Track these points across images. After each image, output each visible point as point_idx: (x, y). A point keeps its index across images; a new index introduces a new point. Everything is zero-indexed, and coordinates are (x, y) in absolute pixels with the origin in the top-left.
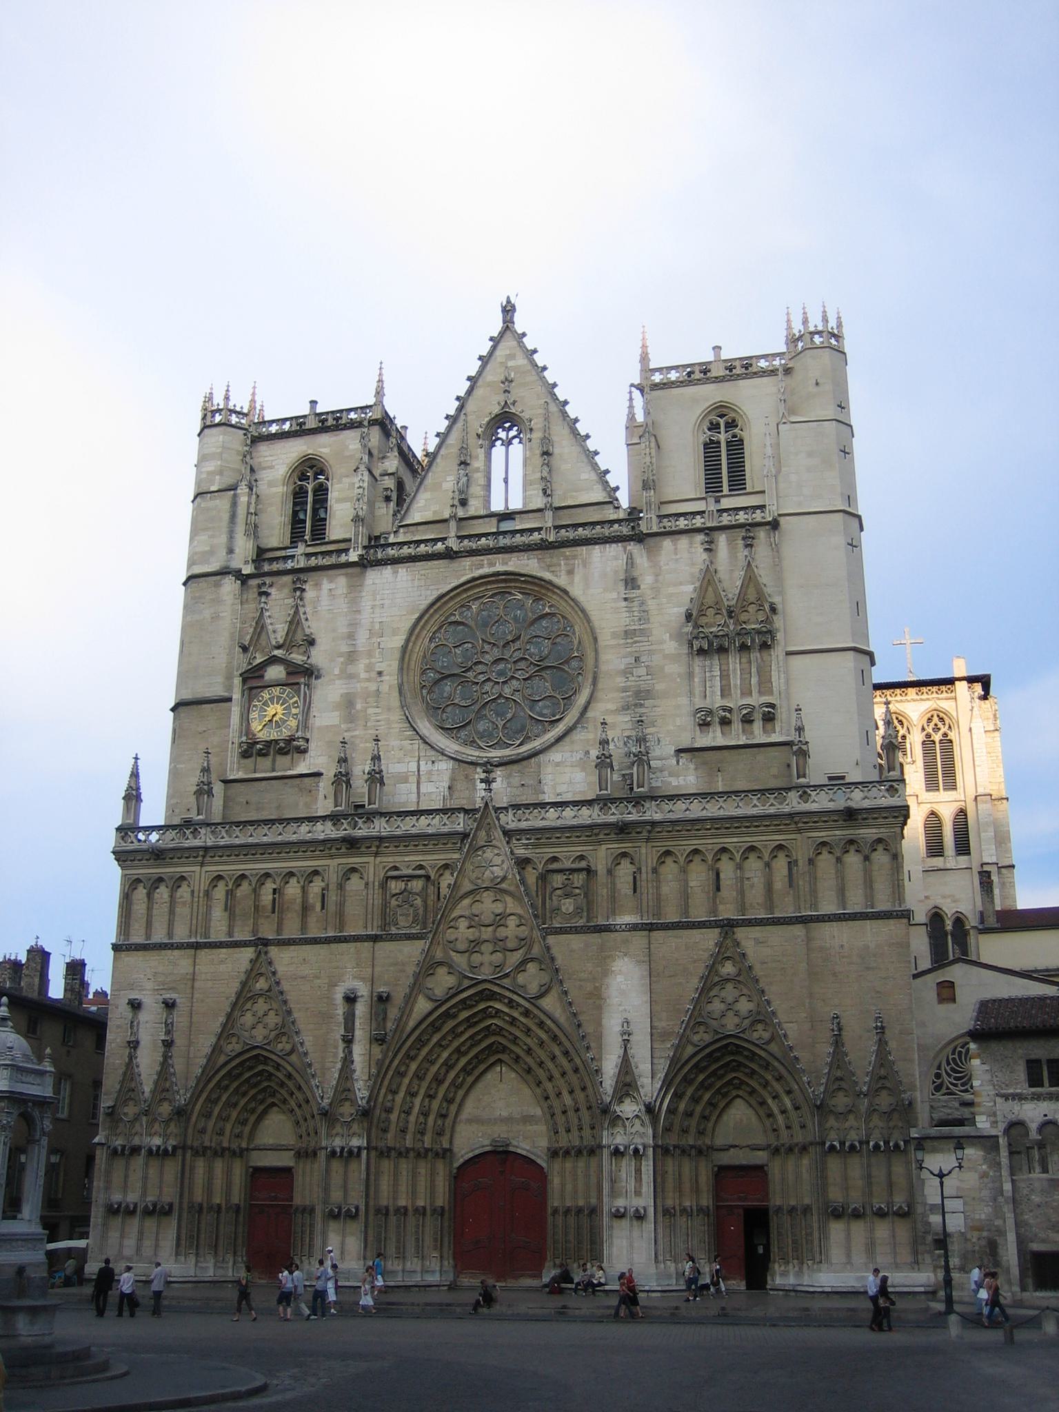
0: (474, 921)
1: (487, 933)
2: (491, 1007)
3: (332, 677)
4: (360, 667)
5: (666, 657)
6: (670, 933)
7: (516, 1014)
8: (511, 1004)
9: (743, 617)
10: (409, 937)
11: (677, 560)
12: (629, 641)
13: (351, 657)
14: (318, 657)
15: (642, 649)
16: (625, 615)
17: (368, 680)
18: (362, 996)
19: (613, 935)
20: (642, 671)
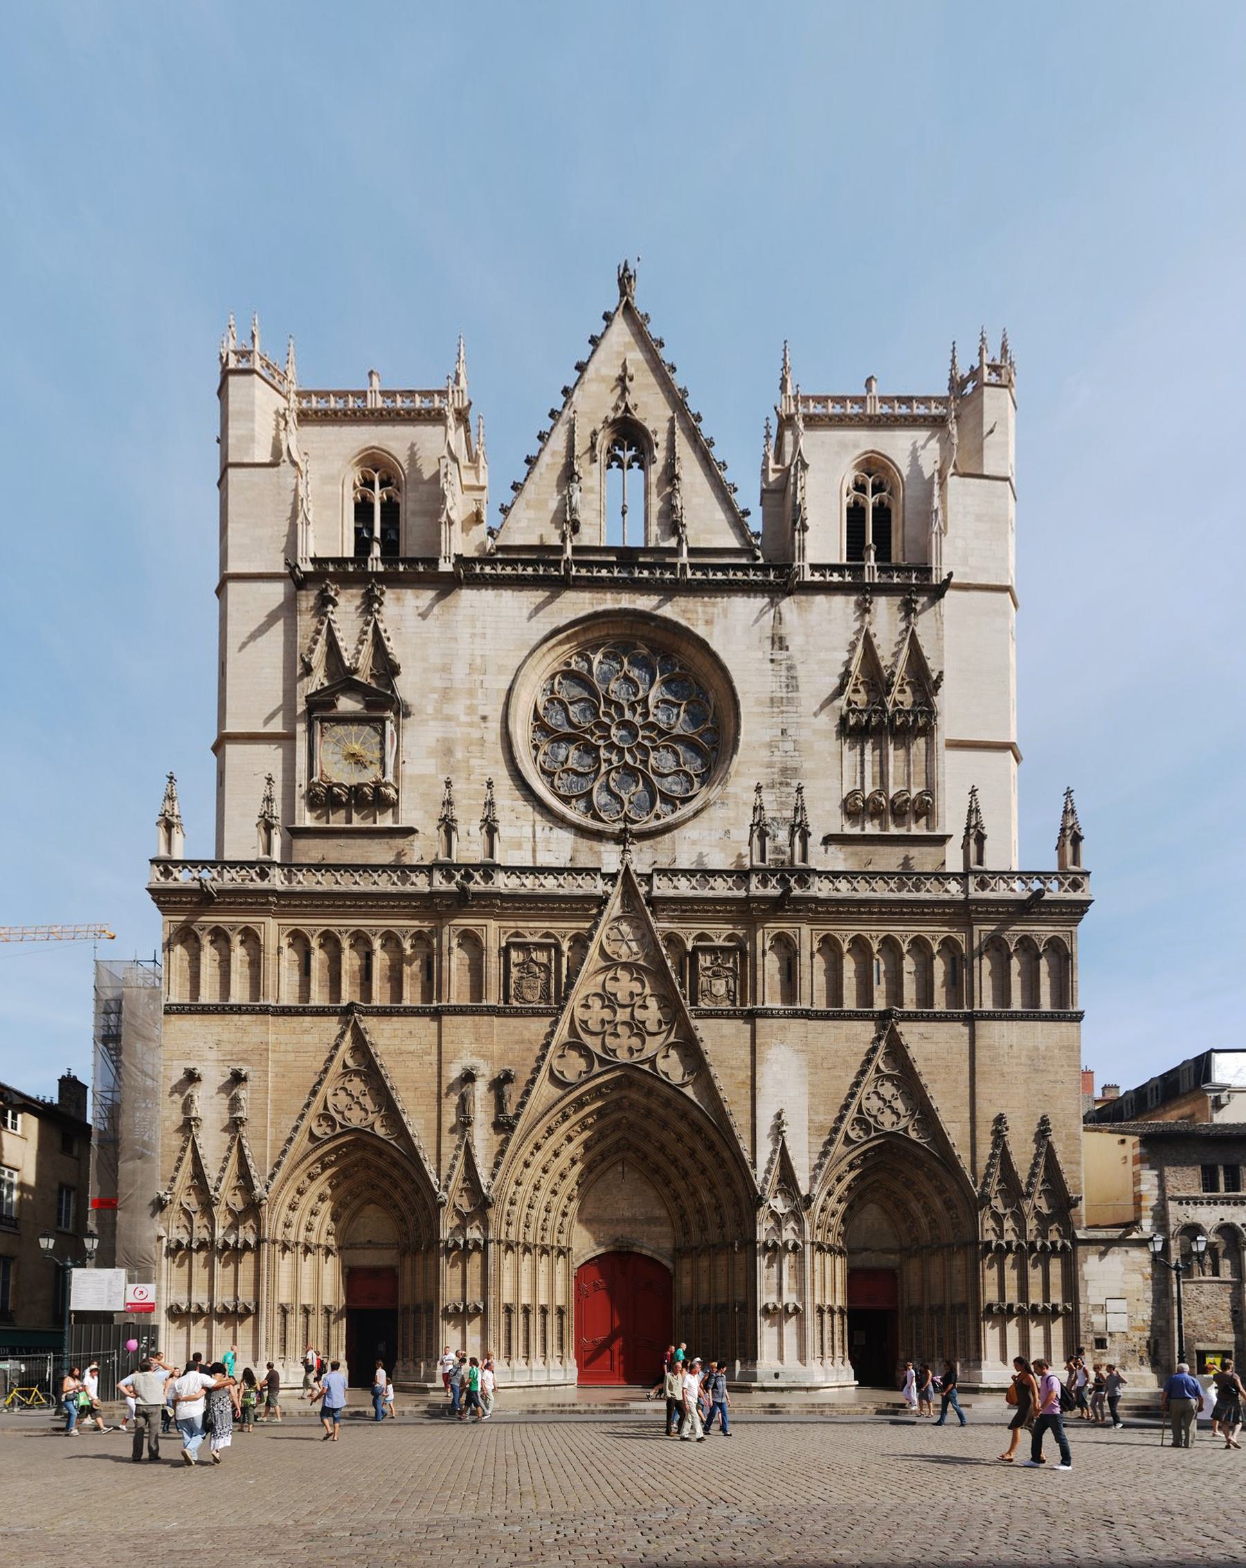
0: (609, 1001)
1: (623, 1015)
2: (625, 1097)
3: (425, 717)
4: (458, 708)
5: (815, 732)
6: (830, 1023)
7: (654, 1106)
8: (650, 1092)
9: (899, 697)
10: (536, 1013)
11: (830, 620)
12: (776, 710)
13: (446, 694)
14: (405, 686)
15: (790, 720)
16: (770, 678)
17: (471, 725)
18: (483, 1075)
19: (769, 1021)
20: (789, 746)
